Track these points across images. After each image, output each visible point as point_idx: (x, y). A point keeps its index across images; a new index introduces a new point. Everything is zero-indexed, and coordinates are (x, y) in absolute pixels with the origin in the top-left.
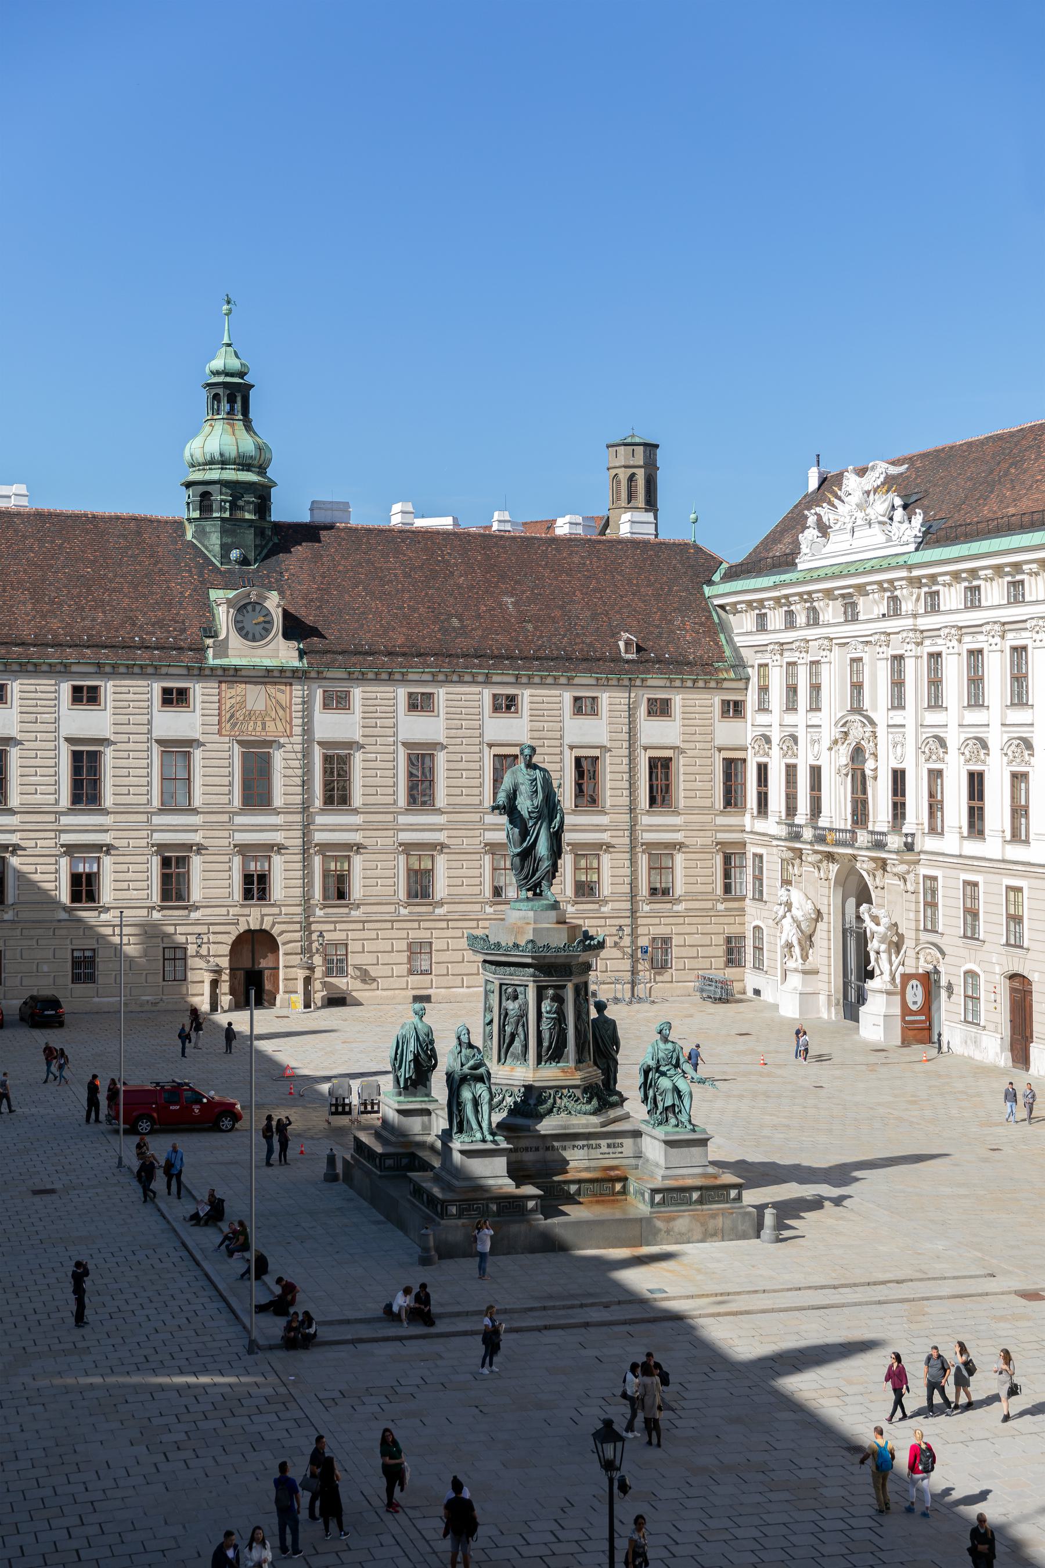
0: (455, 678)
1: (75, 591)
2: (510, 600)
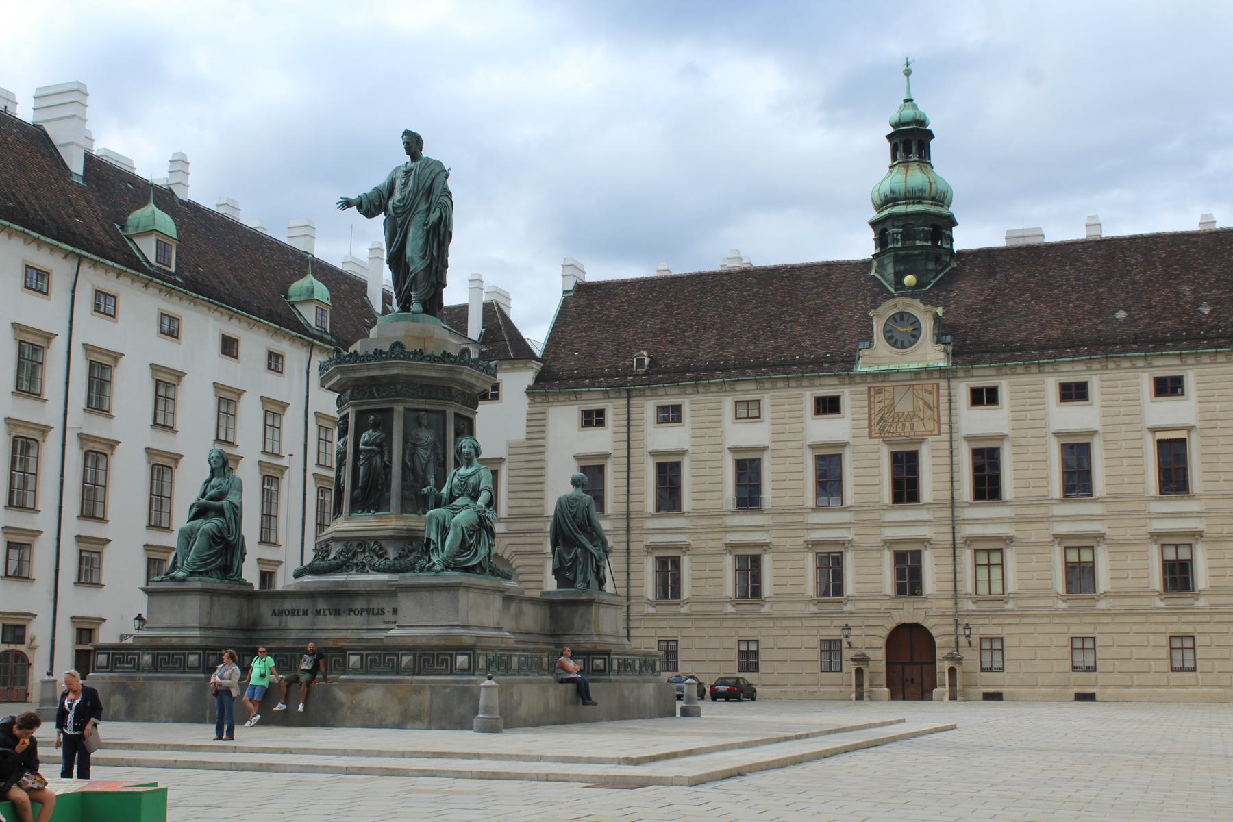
0: (1111, 365)
1: (755, 327)
2: (1188, 289)
